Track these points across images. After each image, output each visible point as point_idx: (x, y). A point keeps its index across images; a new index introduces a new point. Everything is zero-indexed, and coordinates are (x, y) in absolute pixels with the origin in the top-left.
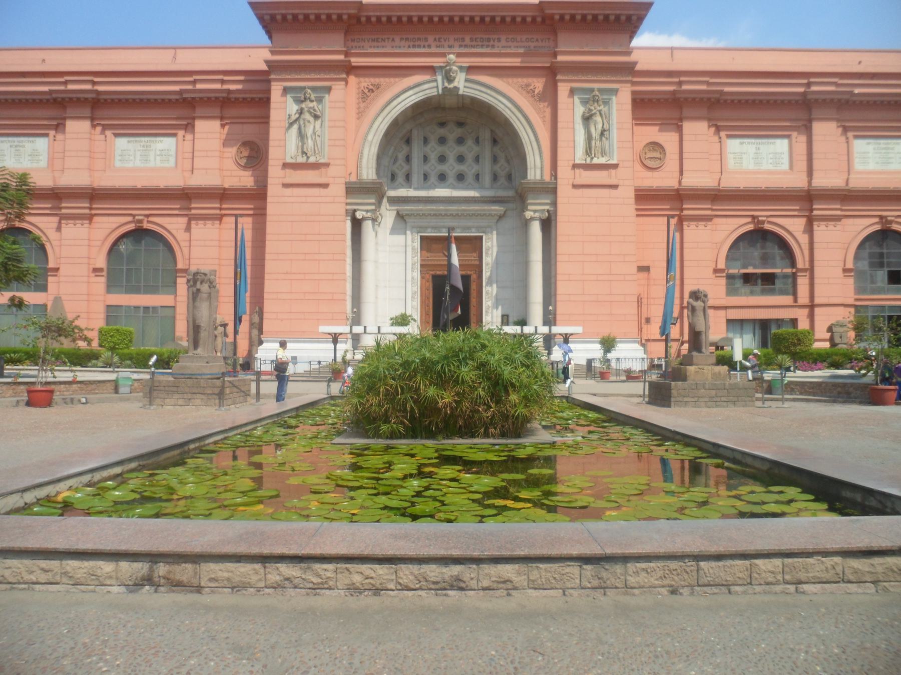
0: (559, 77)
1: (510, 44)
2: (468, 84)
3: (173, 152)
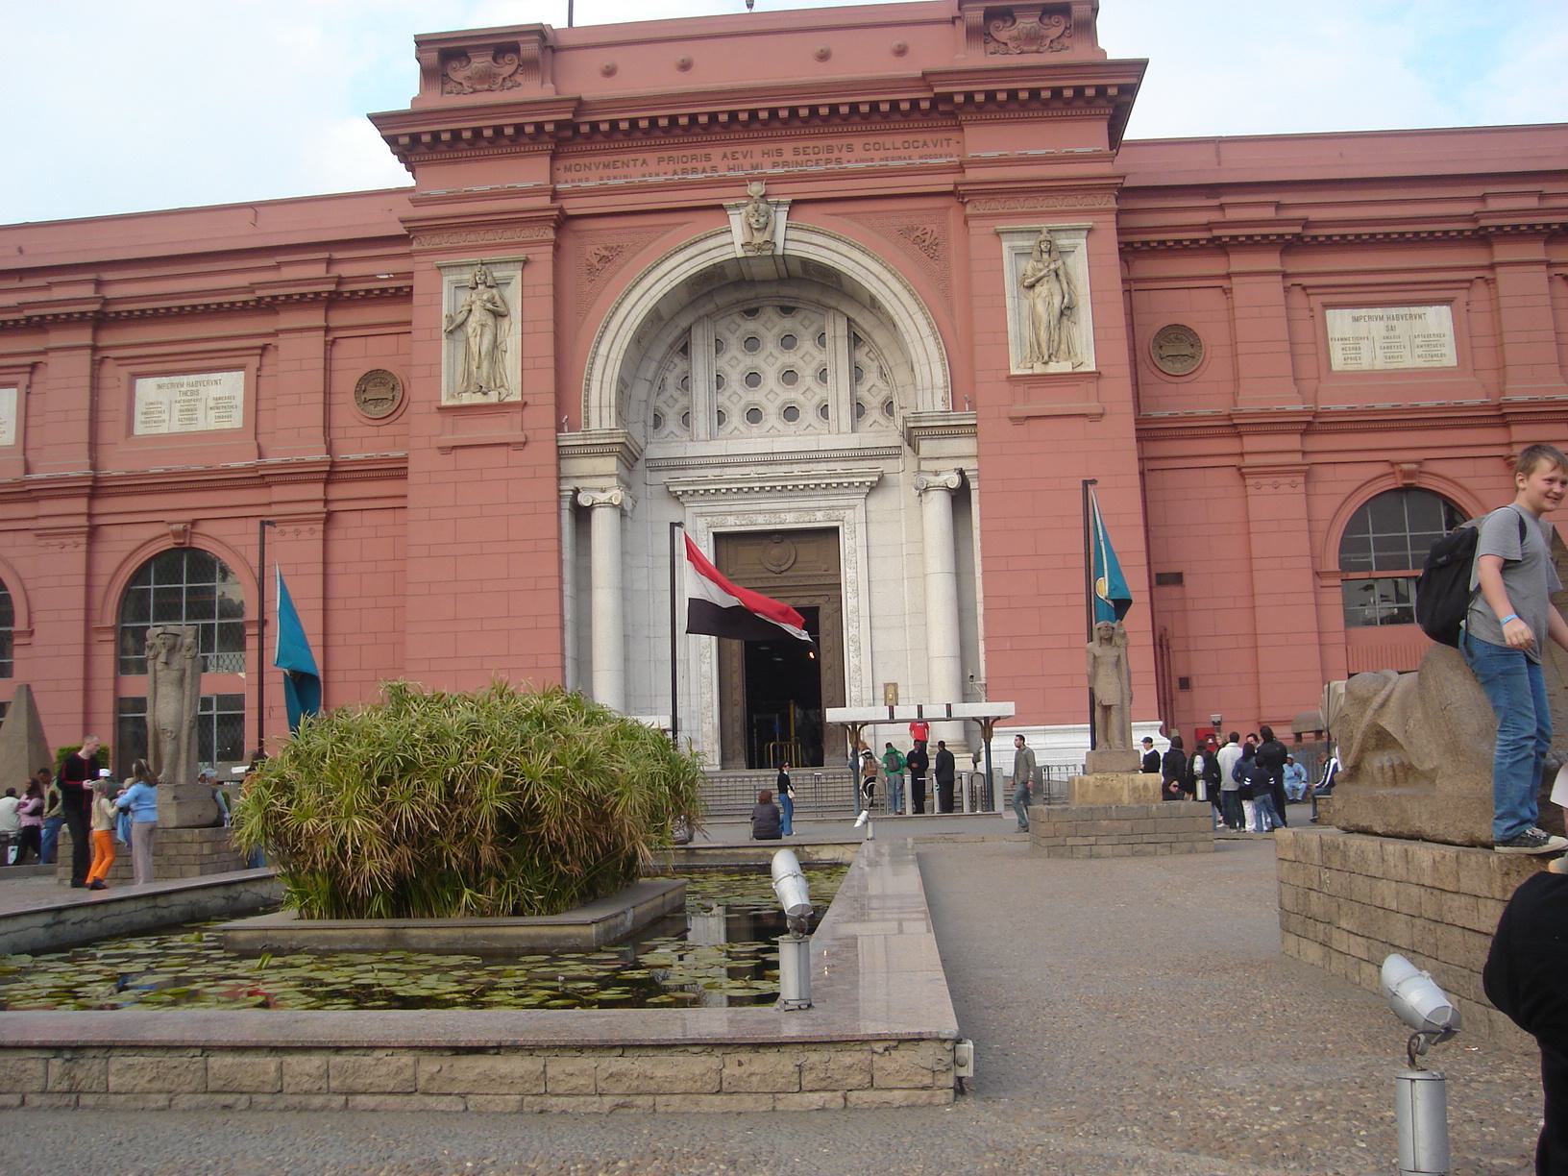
0: (969, 210)
1: (872, 154)
2: (792, 234)
3: (239, 400)
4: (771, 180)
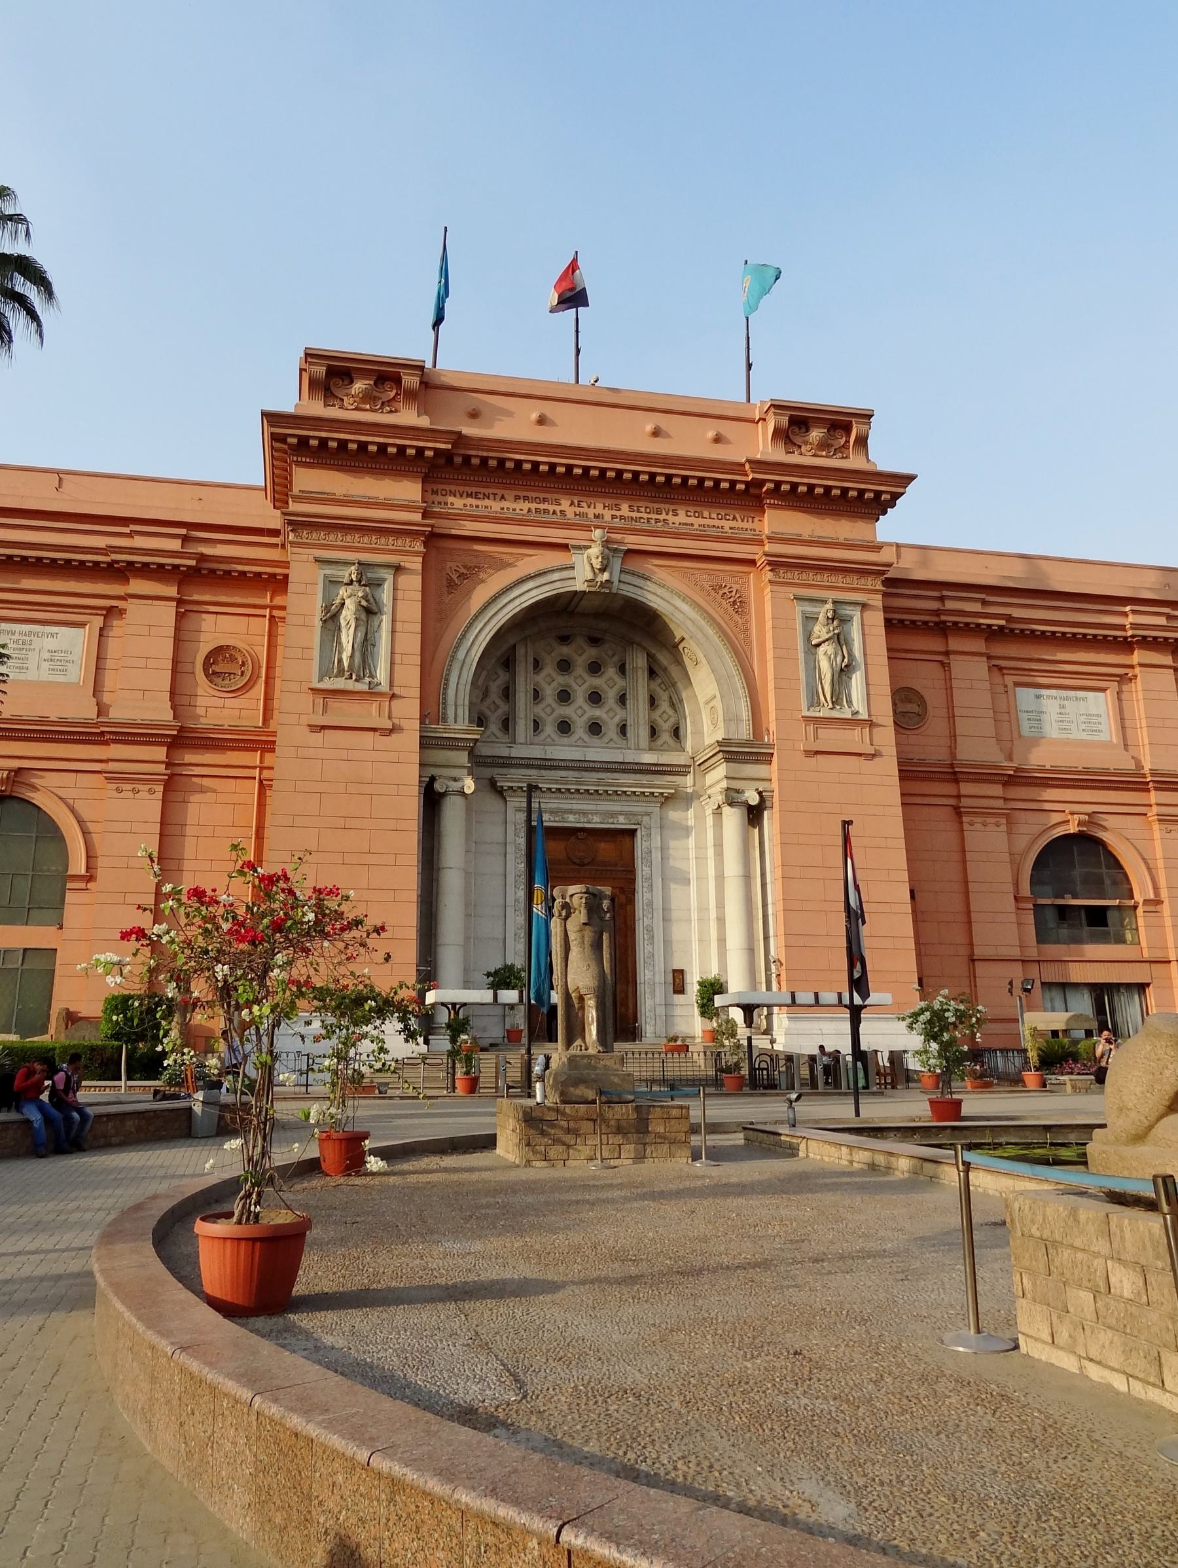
4: (612, 530)
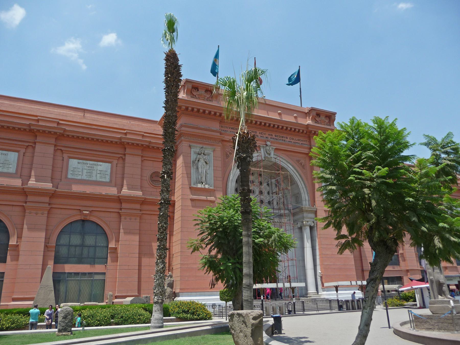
1: (291, 140)
